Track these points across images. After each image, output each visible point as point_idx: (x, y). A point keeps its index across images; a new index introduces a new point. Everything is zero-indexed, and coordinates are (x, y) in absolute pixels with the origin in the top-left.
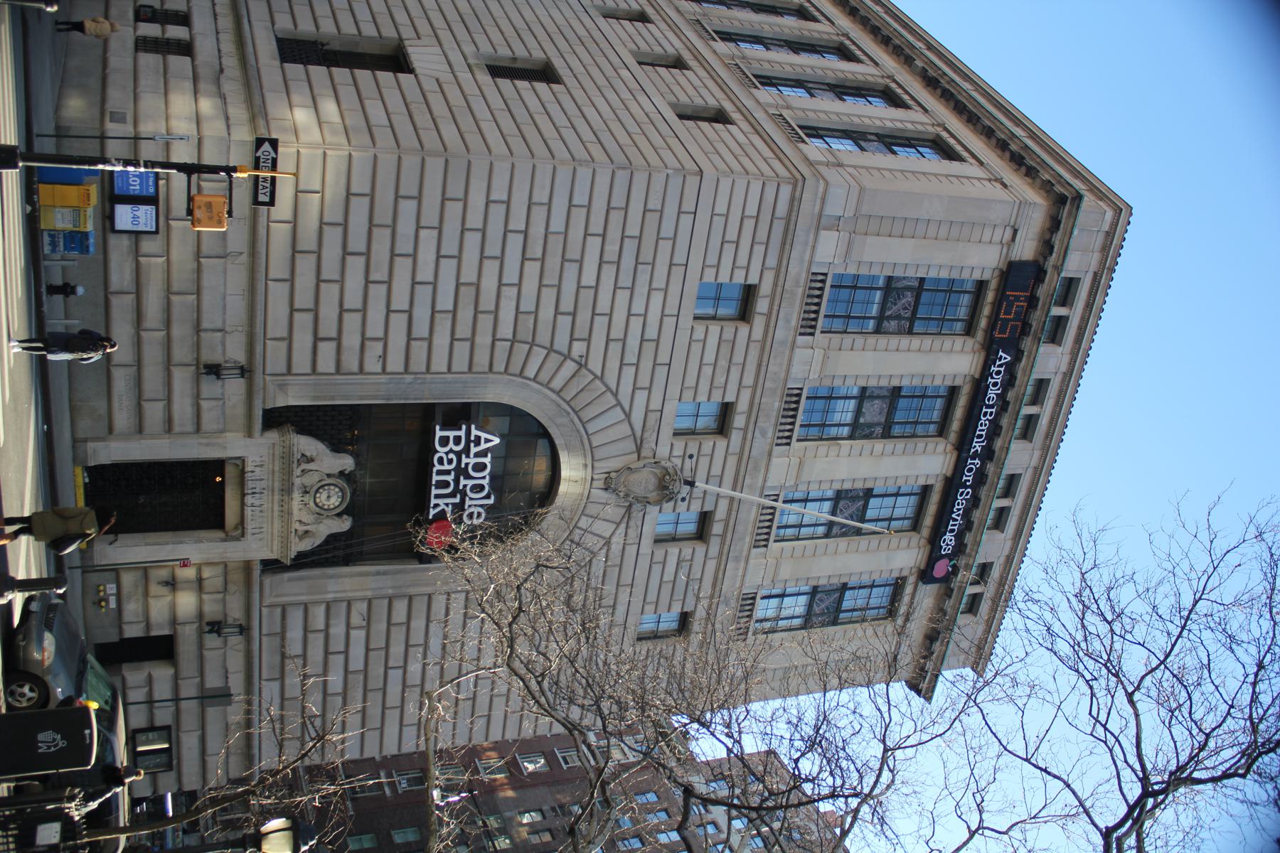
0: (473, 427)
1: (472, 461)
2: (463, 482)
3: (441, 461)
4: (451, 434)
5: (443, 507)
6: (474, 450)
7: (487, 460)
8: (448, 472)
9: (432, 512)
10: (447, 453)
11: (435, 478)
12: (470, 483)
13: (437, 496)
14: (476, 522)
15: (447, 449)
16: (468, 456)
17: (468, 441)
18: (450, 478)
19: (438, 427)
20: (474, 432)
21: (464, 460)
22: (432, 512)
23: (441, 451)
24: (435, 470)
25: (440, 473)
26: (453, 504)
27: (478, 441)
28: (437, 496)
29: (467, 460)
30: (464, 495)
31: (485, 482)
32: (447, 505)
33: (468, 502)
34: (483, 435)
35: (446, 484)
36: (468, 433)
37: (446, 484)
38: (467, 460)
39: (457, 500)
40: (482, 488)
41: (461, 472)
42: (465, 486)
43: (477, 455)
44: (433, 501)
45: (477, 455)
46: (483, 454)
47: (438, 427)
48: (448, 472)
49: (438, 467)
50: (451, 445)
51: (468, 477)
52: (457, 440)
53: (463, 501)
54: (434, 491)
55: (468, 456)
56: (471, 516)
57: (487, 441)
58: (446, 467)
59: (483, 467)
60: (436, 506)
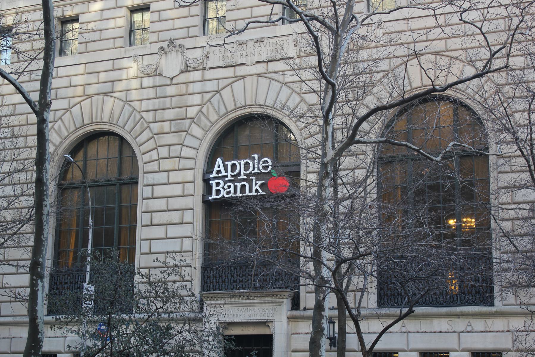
0: (211, 176)
1: (230, 173)
2: (242, 177)
3: (228, 193)
4: (214, 188)
5: (257, 187)
6: (223, 173)
7: (229, 164)
8: (236, 187)
9: (261, 193)
10: (224, 189)
11: (239, 194)
12: (243, 171)
13: (251, 191)
14: (270, 163)
15: (222, 190)
16: (227, 176)
17: (218, 178)
18: (239, 185)
19: (210, 198)
20: (214, 175)
21: (229, 178)
22: (261, 193)
23: (223, 193)
24: (233, 195)
25: (236, 192)
26: (256, 181)
27: (219, 172)
28: (251, 191)
29: (229, 176)
30: (251, 174)
31: (243, 163)
32: (256, 184)
33: (256, 171)
34: (216, 168)
35: (243, 187)
36: (215, 178)
37: (243, 187)
38: (229, 176)
39: (254, 178)
40: (247, 164)
41: (235, 178)
42: (245, 175)
43: (226, 171)
44: (254, 193)
45: (226, 171)
46: (226, 167)
47: (210, 198)
48: (236, 187)
49: (232, 194)
50: (219, 188)
51: (239, 174)
52: (218, 184)
53: (255, 174)
54: (247, 193)
55: (227, 176)
56: (265, 168)
57: (219, 167)
58: (232, 189)
59: (234, 165)
60: (257, 191)
